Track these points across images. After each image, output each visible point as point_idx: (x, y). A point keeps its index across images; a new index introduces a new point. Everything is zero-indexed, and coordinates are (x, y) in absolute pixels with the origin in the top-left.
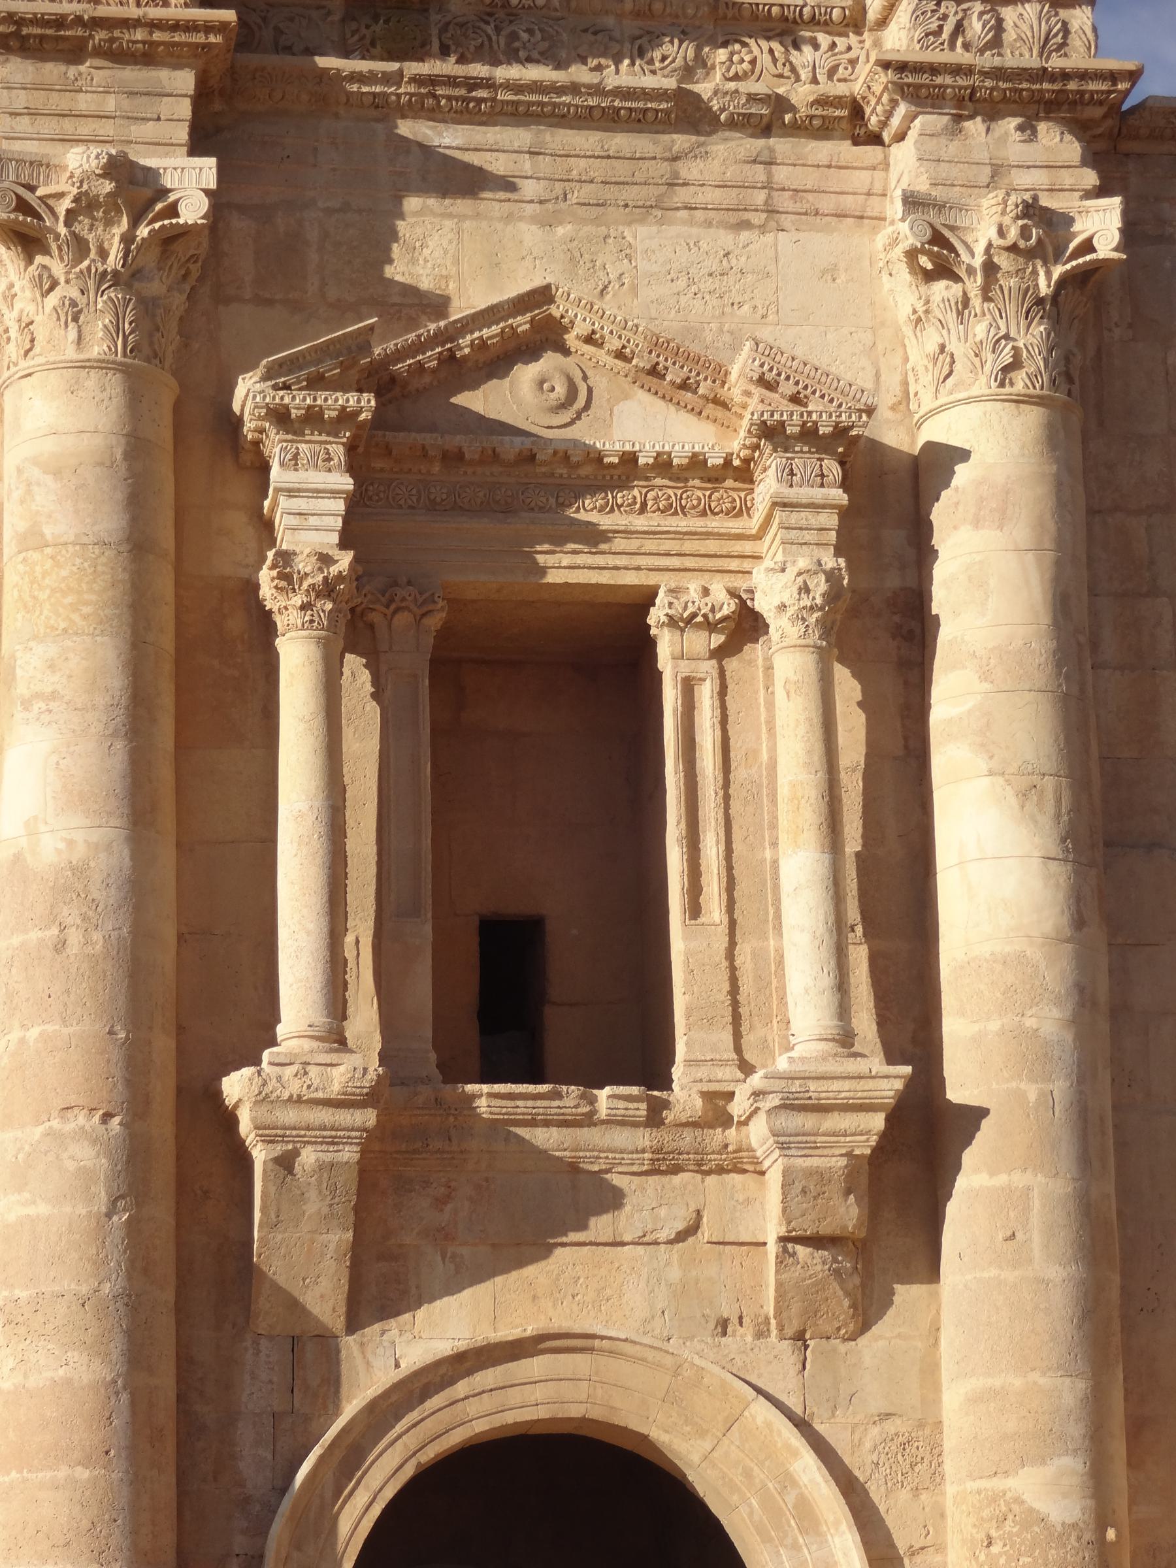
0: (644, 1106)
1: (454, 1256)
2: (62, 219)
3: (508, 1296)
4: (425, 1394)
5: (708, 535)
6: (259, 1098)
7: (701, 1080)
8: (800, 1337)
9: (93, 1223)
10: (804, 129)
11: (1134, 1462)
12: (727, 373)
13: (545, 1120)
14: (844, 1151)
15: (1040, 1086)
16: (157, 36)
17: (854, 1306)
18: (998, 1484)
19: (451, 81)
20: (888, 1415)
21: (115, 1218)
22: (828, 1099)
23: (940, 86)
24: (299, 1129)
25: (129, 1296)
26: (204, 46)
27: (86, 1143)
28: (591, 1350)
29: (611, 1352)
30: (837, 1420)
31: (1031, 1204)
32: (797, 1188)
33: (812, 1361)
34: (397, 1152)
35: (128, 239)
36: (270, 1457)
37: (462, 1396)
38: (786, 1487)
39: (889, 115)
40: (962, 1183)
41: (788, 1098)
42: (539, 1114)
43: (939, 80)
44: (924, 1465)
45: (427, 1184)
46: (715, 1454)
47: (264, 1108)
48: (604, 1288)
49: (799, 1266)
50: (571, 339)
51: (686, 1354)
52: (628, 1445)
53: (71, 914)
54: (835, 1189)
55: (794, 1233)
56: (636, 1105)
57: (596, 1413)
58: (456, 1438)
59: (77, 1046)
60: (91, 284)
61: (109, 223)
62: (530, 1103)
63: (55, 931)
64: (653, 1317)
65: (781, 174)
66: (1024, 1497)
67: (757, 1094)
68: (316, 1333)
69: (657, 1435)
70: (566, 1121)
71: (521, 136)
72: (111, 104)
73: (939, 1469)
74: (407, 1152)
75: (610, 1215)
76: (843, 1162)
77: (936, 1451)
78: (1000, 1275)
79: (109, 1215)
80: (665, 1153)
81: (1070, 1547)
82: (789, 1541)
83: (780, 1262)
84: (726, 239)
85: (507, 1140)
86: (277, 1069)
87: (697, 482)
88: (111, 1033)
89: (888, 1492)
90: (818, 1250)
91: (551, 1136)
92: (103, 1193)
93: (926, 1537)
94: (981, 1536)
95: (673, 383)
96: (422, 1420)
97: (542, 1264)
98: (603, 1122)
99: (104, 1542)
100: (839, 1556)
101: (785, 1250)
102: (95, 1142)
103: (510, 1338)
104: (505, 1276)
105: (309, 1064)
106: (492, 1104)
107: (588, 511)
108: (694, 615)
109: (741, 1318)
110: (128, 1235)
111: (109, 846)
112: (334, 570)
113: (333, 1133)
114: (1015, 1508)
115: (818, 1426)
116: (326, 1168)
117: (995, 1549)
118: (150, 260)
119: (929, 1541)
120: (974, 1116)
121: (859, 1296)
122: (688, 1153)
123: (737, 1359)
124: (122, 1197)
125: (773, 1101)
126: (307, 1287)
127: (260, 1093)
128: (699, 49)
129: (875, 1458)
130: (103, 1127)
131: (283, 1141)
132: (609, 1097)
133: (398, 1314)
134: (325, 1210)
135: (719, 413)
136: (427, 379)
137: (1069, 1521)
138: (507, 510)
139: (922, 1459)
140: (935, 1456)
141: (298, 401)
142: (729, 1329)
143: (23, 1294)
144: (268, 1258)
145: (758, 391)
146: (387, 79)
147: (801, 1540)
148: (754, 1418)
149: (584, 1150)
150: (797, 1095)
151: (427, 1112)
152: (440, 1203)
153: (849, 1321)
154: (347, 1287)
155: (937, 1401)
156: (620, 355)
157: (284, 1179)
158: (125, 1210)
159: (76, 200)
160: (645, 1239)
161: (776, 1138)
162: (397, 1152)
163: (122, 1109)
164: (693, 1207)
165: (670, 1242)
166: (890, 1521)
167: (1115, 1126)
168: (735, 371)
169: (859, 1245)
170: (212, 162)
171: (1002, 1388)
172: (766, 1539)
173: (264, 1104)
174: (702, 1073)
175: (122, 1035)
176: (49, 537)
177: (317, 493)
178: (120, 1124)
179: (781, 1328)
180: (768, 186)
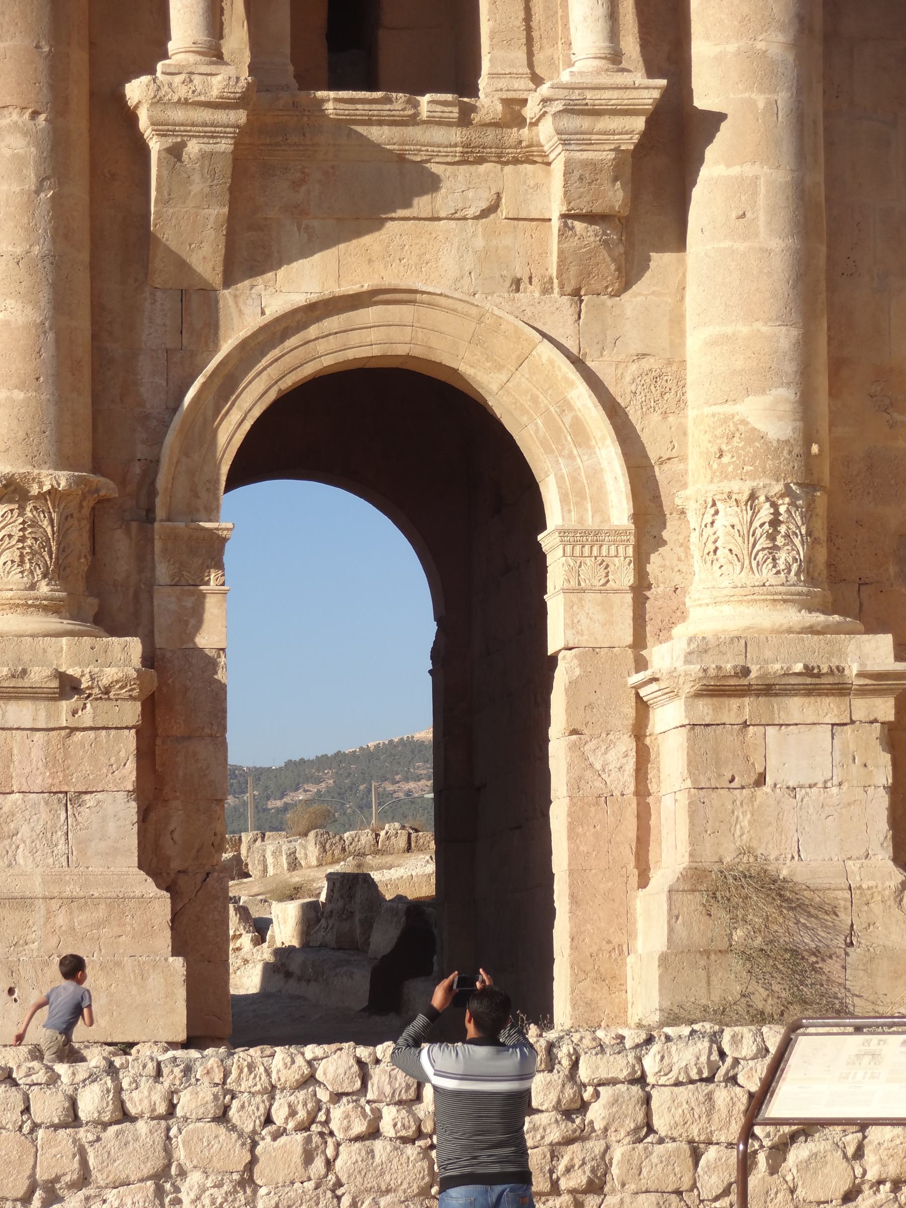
0: (456, 110)
1: (307, 227)
3: (349, 259)
4: (285, 334)
6: (154, 100)
7: (501, 90)
8: (576, 293)
9: (25, 197)
11: (834, 393)
13: (379, 120)
14: (613, 147)
15: (767, 96)
17: (618, 269)
18: (728, 409)
21: (42, 195)
22: (601, 105)
24: (186, 125)
25: (54, 256)
27: (19, 135)
28: (413, 302)
29: (430, 304)
30: (605, 359)
31: (758, 190)
32: (577, 174)
33: (586, 313)
34: (262, 145)
36: (164, 384)
37: (313, 337)
38: (564, 410)
40: (705, 173)
41: (569, 105)
42: (374, 116)
44: (672, 394)
46: (509, 384)
47: (159, 108)
48: (425, 254)
49: (577, 238)
51: (488, 306)
52: (442, 378)
54: (605, 177)
55: (573, 212)
56: (450, 109)
57: (417, 352)
58: (308, 370)
59: (11, 57)
62: (367, 107)
64: (462, 277)
66: (748, 420)
67: (545, 101)
68: (199, 287)
69: (464, 368)
70: (395, 121)
74: (270, 145)
75: (429, 196)
76: (612, 155)
78: (733, 245)
79: (37, 192)
80: (473, 147)
81: (783, 458)
82: (566, 452)
83: (561, 234)
85: (349, 136)
86: (168, 77)
88: (38, 47)
89: (643, 415)
90: (591, 225)
91: (383, 133)
92: (33, 175)
93: (672, 450)
94: (715, 449)
96: (283, 356)
97: (376, 235)
98: (424, 122)
99: (35, 449)
100: (604, 464)
101: (566, 225)
102: (25, 134)
103: (351, 293)
104: (347, 243)
105: (194, 73)
106: (337, 107)
109: (530, 278)
113: (213, 129)
114: (742, 428)
115: (589, 364)
116: (207, 157)
117: (726, 459)
119: (674, 453)
120: (715, 119)
121: (623, 262)
122: (491, 148)
123: (528, 311)
124: (47, 178)
125: (558, 106)
126: (193, 251)
127: (155, 96)
129: (633, 388)
130: (32, 122)
131: (173, 135)
132: (429, 102)
133: (263, 272)
134: (207, 190)
137: (783, 438)
139: (670, 389)
142: (522, 287)
144: (162, 227)
147: (575, 452)
148: (540, 356)
149: (409, 145)
150: (576, 102)
151: (285, 113)
152: (296, 185)
153: (614, 281)
154: (223, 251)
155: (683, 345)
157: (174, 165)
158: (50, 188)
160: (457, 216)
161: (559, 136)
162: (262, 145)
163: (47, 108)
165: (476, 218)
166: (645, 438)
167: (825, 129)
169: (623, 221)
171: (734, 335)
172: (549, 451)
173: (159, 105)
174: (502, 83)
175: (46, 49)
178: (46, 120)
179: (562, 286)
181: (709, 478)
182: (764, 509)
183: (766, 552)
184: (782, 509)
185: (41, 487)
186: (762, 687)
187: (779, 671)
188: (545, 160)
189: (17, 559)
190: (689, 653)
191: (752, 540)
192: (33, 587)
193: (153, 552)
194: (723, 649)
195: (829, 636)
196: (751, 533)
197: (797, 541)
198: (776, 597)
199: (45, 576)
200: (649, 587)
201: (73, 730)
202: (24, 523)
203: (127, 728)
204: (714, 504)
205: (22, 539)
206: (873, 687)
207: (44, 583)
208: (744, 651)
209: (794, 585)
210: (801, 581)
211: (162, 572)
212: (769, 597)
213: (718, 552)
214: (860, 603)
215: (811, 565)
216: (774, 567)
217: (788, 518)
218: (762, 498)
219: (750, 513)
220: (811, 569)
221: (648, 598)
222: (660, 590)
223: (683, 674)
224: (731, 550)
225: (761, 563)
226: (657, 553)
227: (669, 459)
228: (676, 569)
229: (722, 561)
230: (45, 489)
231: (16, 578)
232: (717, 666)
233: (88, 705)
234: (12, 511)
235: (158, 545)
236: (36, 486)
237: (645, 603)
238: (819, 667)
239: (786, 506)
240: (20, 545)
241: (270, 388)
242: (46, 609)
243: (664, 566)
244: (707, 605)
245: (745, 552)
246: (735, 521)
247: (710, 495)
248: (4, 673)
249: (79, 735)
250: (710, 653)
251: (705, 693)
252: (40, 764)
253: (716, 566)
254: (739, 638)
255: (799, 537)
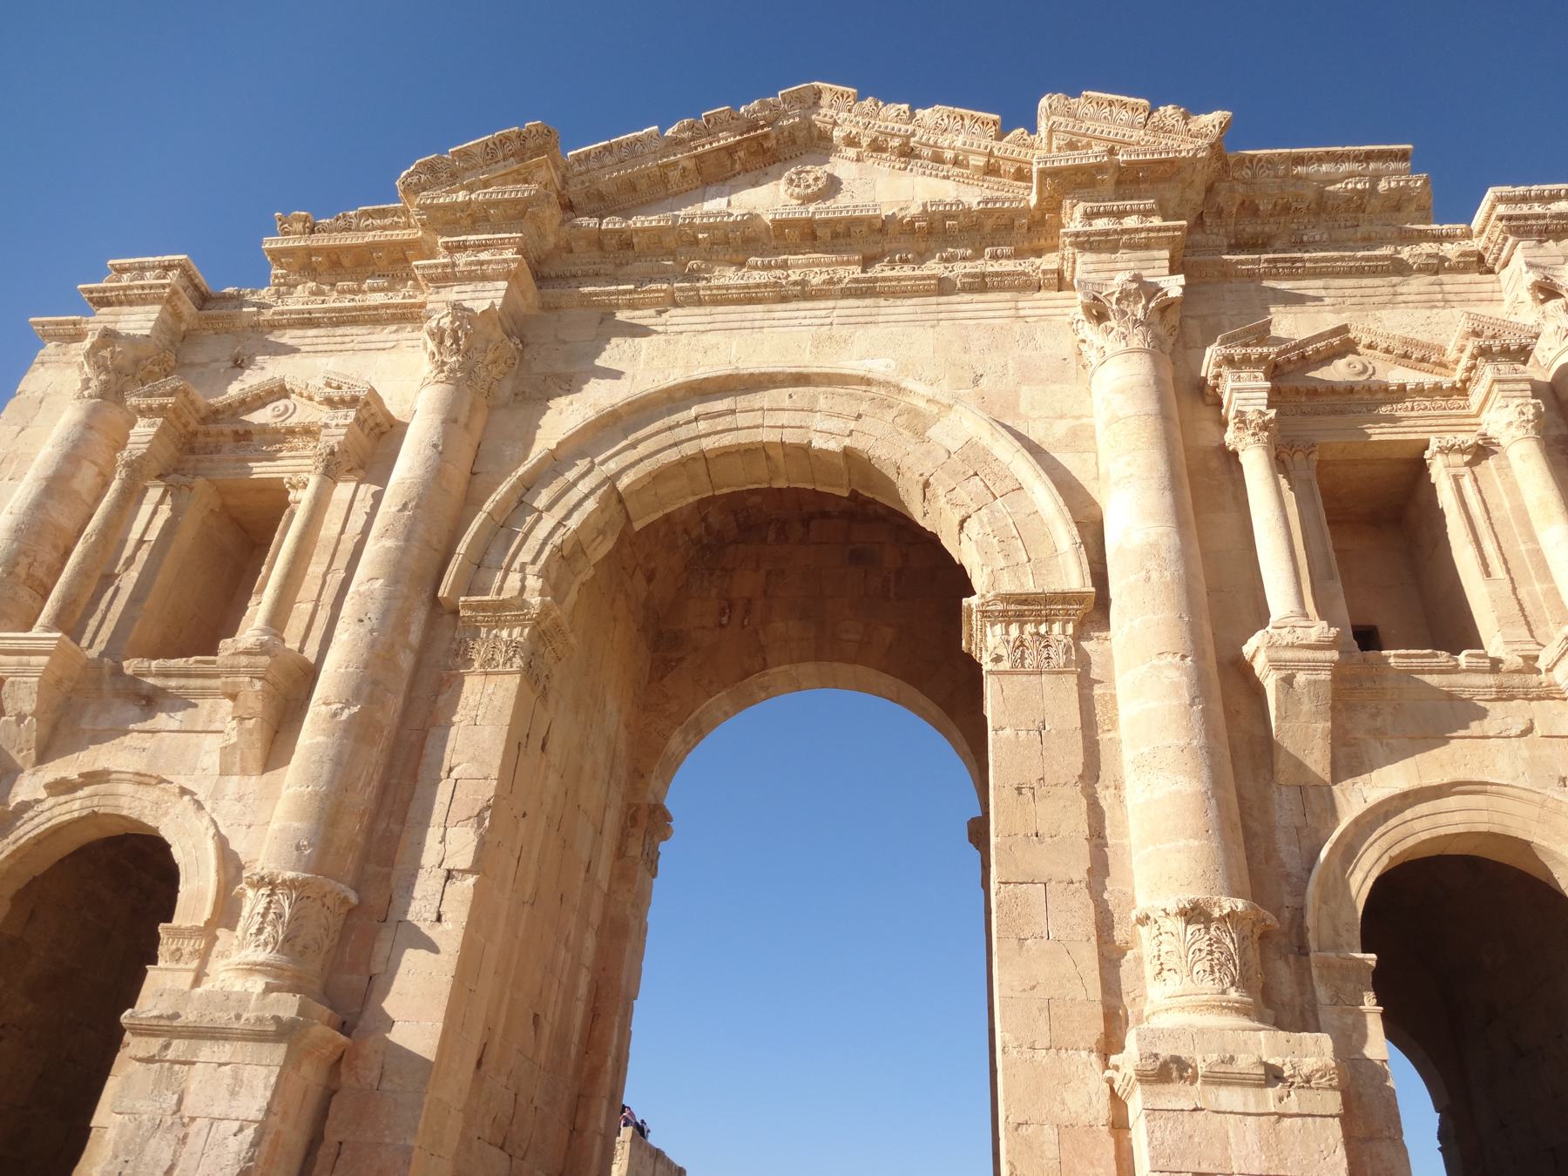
1: (1388, 744)
2: (1114, 303)
4: (1386, 818)
5: (1450, 416)
9: (1183, 709)
10: (1454, 269)
12: (1445, 350)
16: (1152, 235)
19: (1284, 260)
23: (1530, 225)
26: (1173, 237)
28: (1485, 792)
29: (1498, 794)
35: (1145, 308)
39: (1501, 250)
43: (1529, 222)
45: (1364, 707)
50: (1360, 348)
53: (1152, 564)
60: (1130, 325)
61: (1136, 303)
62: (1420, 660)
63: (1144, 573)
65: (1447, 288)
71: (1320, 283)
72: (1132, 265)
79: (1191, 705)
84: (1428, 313)
86: (1278, 631)
87: (1438, 398)
95: (1417, 358)
97: (1443, 748)
98: (1464, 671)
102: (1178, 669)
107: (1384, 410)
108: (1453, 446)
110: (1203, 716)
111: (1168, 535)
112: (1267, 418)
118: (1156, 318)
124: (1196, 697)
128: (1396, 248)
132: (1467, 656)
134: (1314, 709)
135: (1443, 370)
136: (1292, 367)
138: (1342, 413)
141: (1238, 352)
143: (1145, 750)
145: (1472, 339)
146: (1253, 262)
152: (1374, 716)
156: (1387, 351)
159: (1121, 293)
164: (1527, 718)
165: (1518, 736)
168: (1449, 348)
170: (1182, 276)
176: (1121, 416)
177: (1253, 389)
180: (1442, 292)
185: (1221, 911)
188: (1563, 696)
189: (1208, 969)
192: (1224, 992)
193: (1311, 978)
199: (1232, 985)
201: (1281, 1116)
202: (1210, 939)
203: (1331, 1116)
205: (1211, 953)
207: (1233, 990)
211: (1322, 994)
230: (1225, 912)
231: (1209, 987)
233: (1292, 1093)
234: (1199, 930)
235: (1315, 972)
236: (1217, 910)
240: (1210, 957)
241: (1382, 855)
242: (1237, 1011)
248: (1214, 1059)
249: (1287, 1122)
252: (1255, 1148)
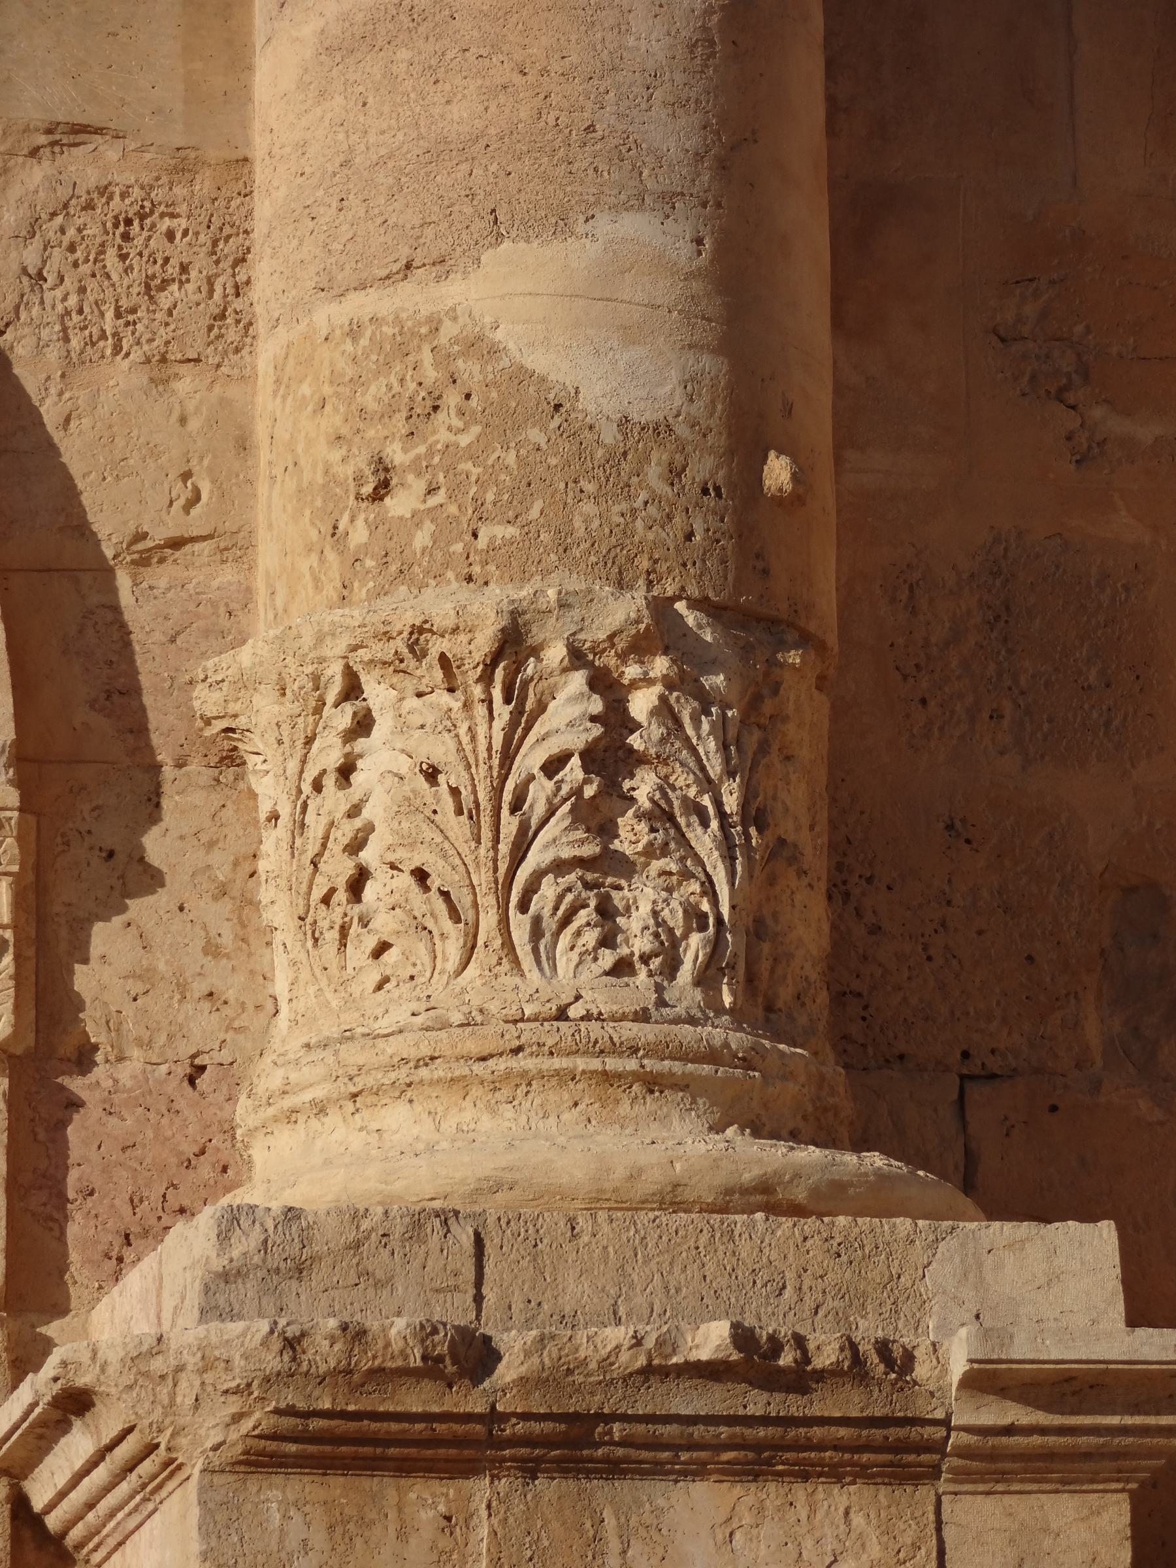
20: (81, 130)
44: (190, 287)
66: (499, 335)
73: (238, 304)
77: (229, 249)
81: (643, 496)
89: (70, 367)
94: (361, 462)
114: (470, 370)
117: (399, 505)
119: (198, 521)
129: (31, 256)
140: (226, 265)
181: (331, 590)
182: (561, 696)
183: (572, 877)
184: (641, 704)
186: (547, 1426)
187: (624, 1357)
190: (225, 1277)
191: (510, 825)
194: (379, 1262)
195: (842, 1220)
196: (507, 797)
197: (705, 841)
198: (613, 1064)
200: (84, 1059)
204: (352, 689)
206: (1036, 1440)
208: (469, 1273)
209: (692, 1021)
210: (720, 1010)
212: (582, 1063)
213: (370, 891)
214: (967, 1152)
215: (766, 947)
216: (607, 941)
217: (663, 740)
218: (555, 653)
219: (503, 713)
220: (764, 967)
221: (74, 1104)
222: (126, 1073)
223: (192, 1361)
224: (421, 876)
225: (550, 924)
226: (117, 921)
227: (176, 544)
228: (199, 988)
229: (384, 924)
232: (344, 1327)
237: (63, 1124)
238: (800, 1341)
239: (658, 689)
243: (146, 975)
244: (320, 1109)
245: (483, 878)
246: (441, 750)
247: (341, 645)
250: (319, 1276)
251: (292, 1448)
253: (362, 943)
254: (446, 1218)
255: (714, 824)
